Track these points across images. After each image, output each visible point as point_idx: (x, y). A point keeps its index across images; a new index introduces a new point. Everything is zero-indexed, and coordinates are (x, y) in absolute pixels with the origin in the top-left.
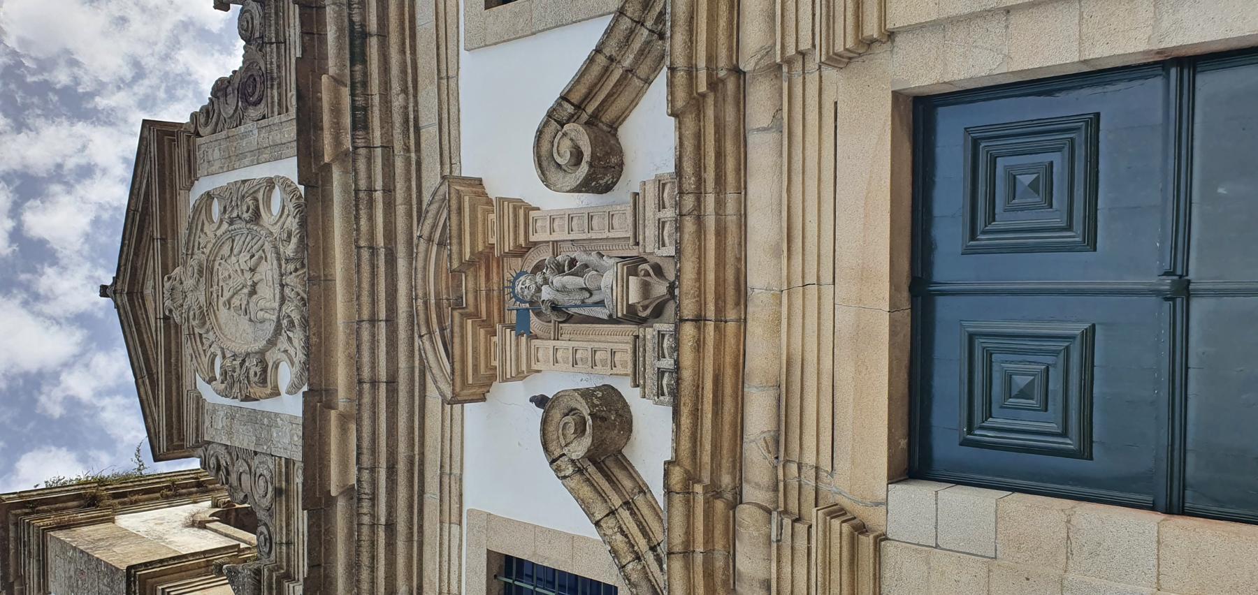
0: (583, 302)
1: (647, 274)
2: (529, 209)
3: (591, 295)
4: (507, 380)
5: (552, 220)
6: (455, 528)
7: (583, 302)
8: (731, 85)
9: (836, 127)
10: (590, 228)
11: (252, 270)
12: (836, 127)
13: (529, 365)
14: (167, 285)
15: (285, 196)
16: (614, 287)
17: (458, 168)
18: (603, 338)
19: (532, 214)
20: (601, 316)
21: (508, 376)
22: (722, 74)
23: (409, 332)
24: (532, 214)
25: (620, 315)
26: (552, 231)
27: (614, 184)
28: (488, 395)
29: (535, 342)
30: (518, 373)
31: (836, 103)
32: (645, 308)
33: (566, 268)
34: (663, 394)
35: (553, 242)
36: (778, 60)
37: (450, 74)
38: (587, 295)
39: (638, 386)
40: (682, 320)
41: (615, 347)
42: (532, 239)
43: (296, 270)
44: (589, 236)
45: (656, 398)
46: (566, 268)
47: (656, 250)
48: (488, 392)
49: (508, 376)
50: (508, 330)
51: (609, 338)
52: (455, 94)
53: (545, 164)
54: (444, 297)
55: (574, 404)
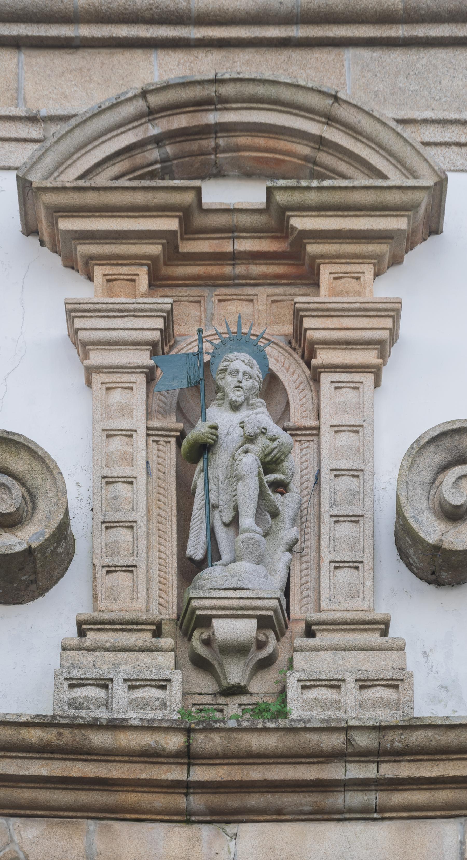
0: (215, 507)
1: (261, 645)
3: (226, 525)
4: (70, 320)
7: (215, 507)
13: (99, 369)
18: (154, 540)
19: (369, 379)
20: (191, 542)
21: (79, 323)
23: (147, 15)
24: (369, 379)
25: (195, 603)
27: (409, 566)
28: (34, 241)
29: (141, 380)
30: (85, 344)
32: (207, 643)
33: (271, 477)
35: (318, 429)
38: (228, 517)
39: (82, 633)
40: (189, 731)
41: (141, 572)
44: (325, 518)
45: (65, 675)
46: (271, 477)
47: (296, 675)
48: (42, 243)
49: (79, 323)
50: (160, 323)
51: (154, 554)
53: (447, 442)
54: (221, 142)
55: (42, 504)
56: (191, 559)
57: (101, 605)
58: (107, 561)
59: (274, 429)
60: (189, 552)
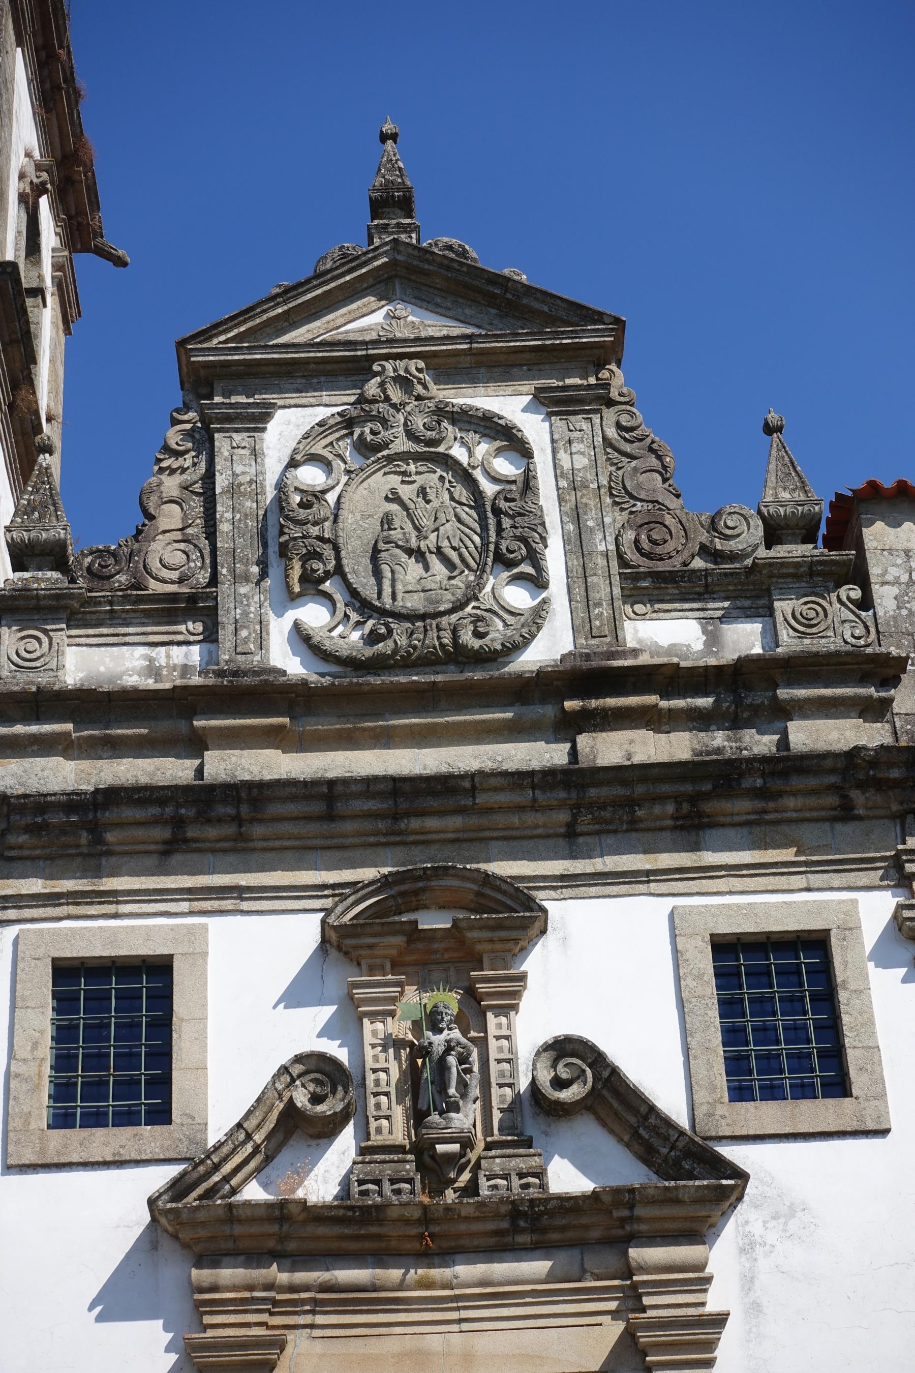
2: (515, 1008)
5: (507, 1038)
6: (184, 906)
8: (620, 1232)
9: (582, 1326)
10: (501, 1086)
11: (439, 552)
12: (582, 1326)
14: (413, 365)
15: (527, 615)
16: (449, 1131)
17: (557, 897)
21: (355, 991)
22: (628, 1228)
26: (498, 1038)
31: (601, 1325)
33: (464, 1066)
34: (359, 1185)
36: (635, 1278)
37: (652, 885)
42: (490, 1016)
43: (442, 645)
52: (631, 892)
56: (421, 1110)
57: (372, 1137)
58: (375, 1114)
59: (464, 1040)
60: (419, 1106)
